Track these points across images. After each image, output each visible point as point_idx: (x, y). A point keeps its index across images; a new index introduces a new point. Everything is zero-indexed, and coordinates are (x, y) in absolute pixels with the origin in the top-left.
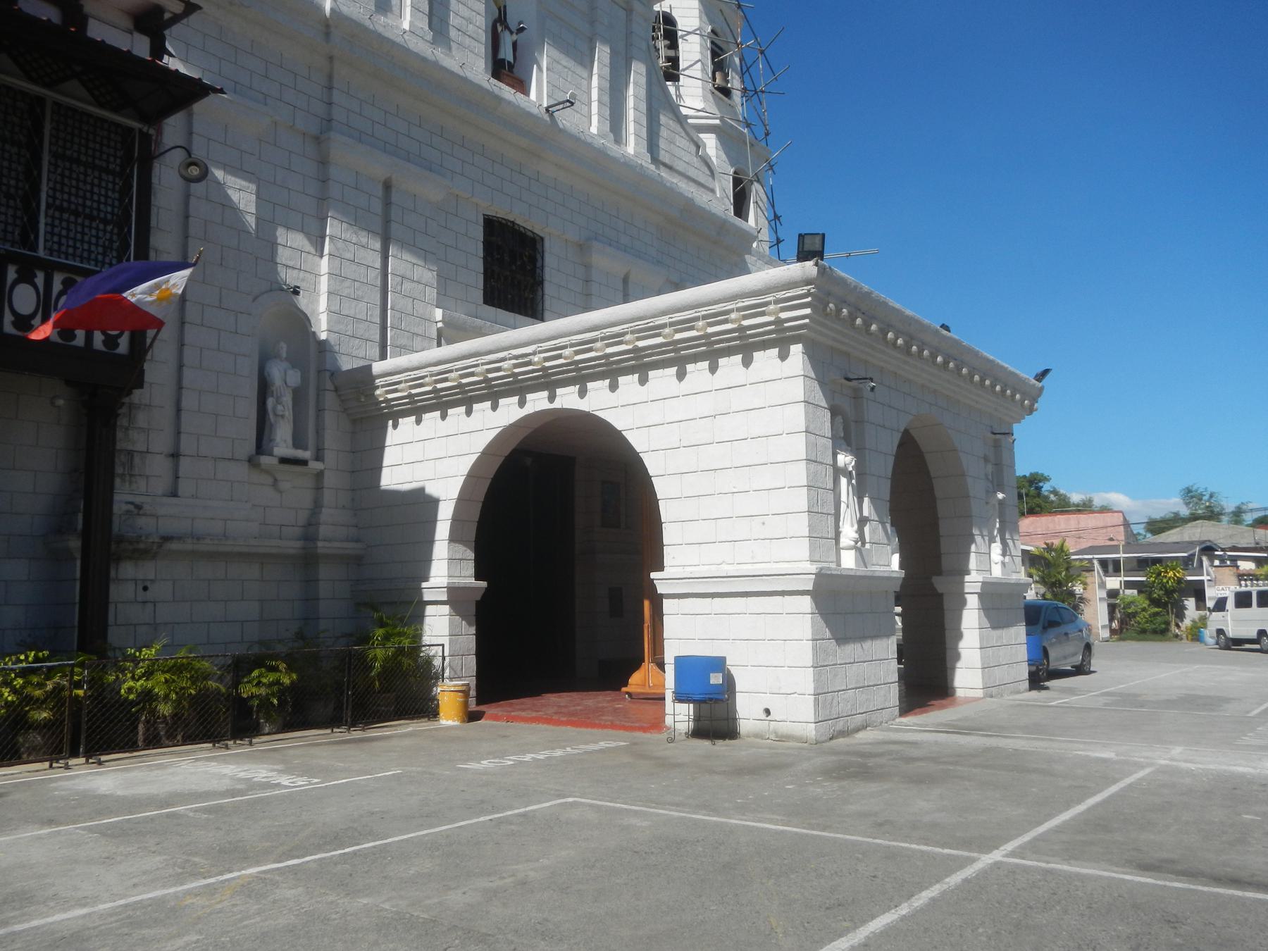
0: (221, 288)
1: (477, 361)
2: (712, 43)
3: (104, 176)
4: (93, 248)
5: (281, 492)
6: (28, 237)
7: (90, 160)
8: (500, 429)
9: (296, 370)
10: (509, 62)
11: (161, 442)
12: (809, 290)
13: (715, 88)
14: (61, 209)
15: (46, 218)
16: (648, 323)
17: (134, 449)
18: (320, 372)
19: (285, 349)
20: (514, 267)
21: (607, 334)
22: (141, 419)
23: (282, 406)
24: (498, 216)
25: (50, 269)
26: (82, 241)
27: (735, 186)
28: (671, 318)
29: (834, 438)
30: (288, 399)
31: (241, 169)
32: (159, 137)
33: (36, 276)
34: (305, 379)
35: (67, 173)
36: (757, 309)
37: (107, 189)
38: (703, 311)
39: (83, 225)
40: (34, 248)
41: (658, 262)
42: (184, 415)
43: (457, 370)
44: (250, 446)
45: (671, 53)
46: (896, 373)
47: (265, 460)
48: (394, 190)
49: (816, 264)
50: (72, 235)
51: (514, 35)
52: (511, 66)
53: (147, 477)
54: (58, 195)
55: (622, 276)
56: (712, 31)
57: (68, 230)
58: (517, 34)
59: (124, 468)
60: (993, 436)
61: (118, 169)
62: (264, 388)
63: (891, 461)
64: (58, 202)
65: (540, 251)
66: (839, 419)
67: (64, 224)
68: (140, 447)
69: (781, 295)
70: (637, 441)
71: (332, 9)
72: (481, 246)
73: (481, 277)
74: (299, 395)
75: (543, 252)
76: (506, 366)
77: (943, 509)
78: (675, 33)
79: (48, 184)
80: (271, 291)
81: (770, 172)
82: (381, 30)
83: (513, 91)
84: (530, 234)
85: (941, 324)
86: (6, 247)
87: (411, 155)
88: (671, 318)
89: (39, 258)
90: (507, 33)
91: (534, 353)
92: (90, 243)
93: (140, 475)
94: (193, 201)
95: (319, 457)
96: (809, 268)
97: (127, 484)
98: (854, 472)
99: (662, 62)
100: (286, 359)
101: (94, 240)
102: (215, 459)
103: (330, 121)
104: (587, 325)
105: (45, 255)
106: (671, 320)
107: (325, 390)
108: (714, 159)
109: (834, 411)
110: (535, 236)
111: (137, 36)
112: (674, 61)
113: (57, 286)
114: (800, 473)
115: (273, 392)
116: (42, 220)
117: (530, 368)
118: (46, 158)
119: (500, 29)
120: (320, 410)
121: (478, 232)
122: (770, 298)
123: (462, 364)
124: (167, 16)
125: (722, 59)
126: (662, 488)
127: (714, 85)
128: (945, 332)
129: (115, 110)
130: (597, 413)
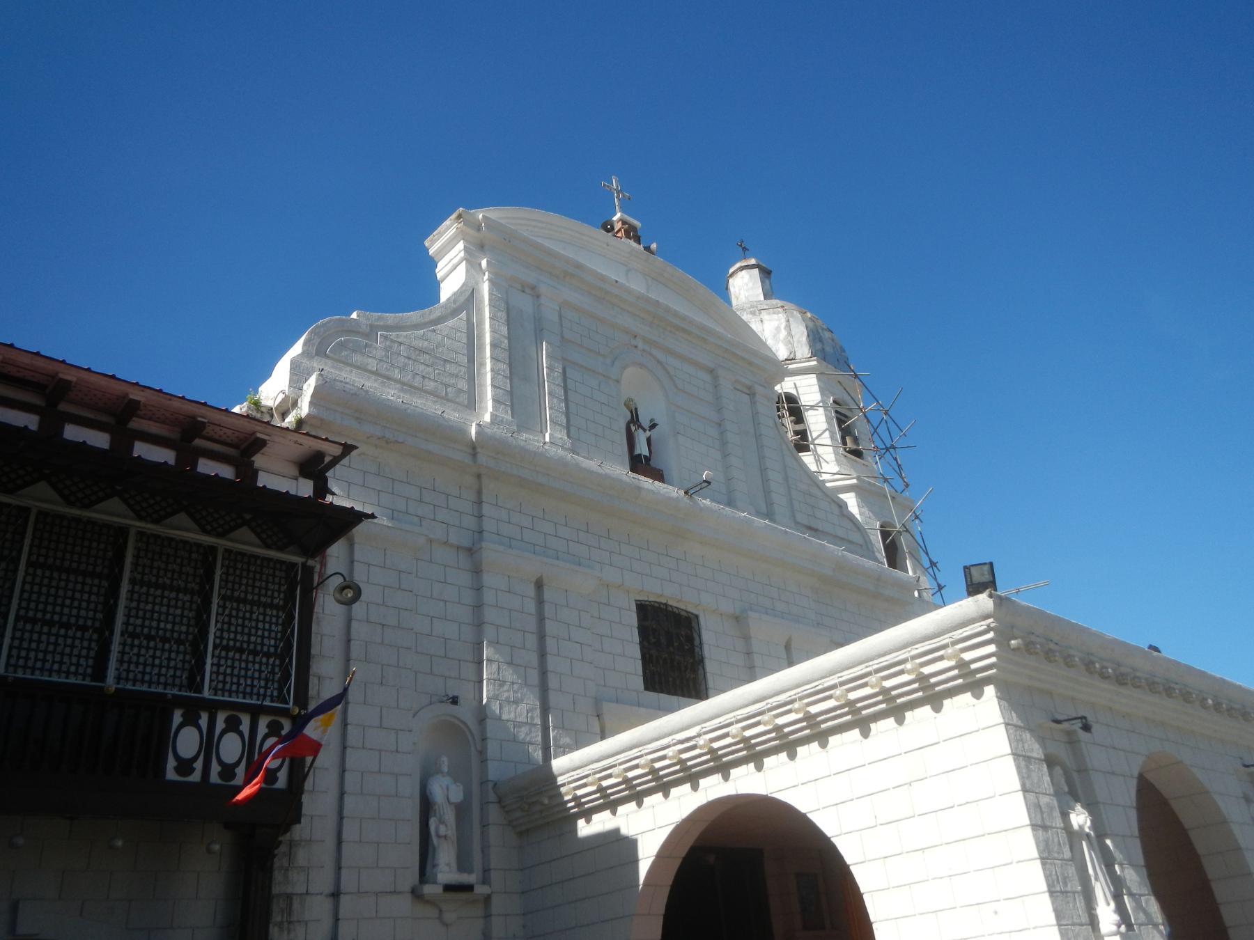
0: (381, 708)
1: (640, 751)
2: (837, 412)
3: (269, 612)
4: (256, 682)
5: (446, 925)
7: (256, 598)
8: (673, 826)
9: (458, 784)
10: (645, 456)
11: (322, 881)
12: (988, 626)
13: (848, 452)
14: (227, 648)
15: (212, 658)
16: (816, 686)
17: (294, 892)
18: (483, 783)
19: (446, 763)
20: (671, 649)
21: (774, 704)
22: (301, 857)
23: (444, 826)
24: (650, 600)
25: (213, 707)
26: (246, 677)
27: (884, 540)
28: (841, 677)
29: (1057, 794)
30: (450, 816)
31: (400, 588)
32: (323, 569)
33: (200, 717)
35: (234, 613)
36: (934, 654)
37: (271, 623)
38: (875, 665)
39: (247, 662)
40: (199, 689)
41: (818, 624)
42: (345, 847)
43: (621, 764)
44: (412, 876)
45: (799, 427)
46: (1110, 709)
47: (428, 889)
48: (545, 588)
49: (991, 596)
50: (236, 672)
51: (647, 432)
52: (648, 459)
53: (306, 923)
54: (225, 635)
55: (784, 644)
56: (835, 402)
57: (233, 667)
58: (650, 430)
59: (283, 916)
60: (1246, 769)
61: (281, 602)
62: (426, 807)
63: (1133, 814)
64: (225, 642)
65: (697, 629)
66: (1058, 770)
67: (229, 663)
68: (300, 889)
69: (958, 634)
70: (826, 823)
71: (476, 433)
72: (636, 632)
73: (639, 664)
74: (462, 811)
75: (699, 629)
76: (671, 754)
77: (1212, 868)
78: (799, 409)
79: (216, 626)
80: (431, 704)
81: (917, 521)
82: (522, 444)
83: (651, 481)
84: (683, 613)
85: (1148, 645)
86: (172, 692)
87: (559, 553)
88: (841, 677)
89: (204, 699)
90: (640, 431)
91: (699, 735)
92: (253, 678)
93: (299, 921)
94: (354, 624)
95: (485, 881)
96: (983, 601)
97: (286, 932)
98: (1092, 833)
99: (790, 436)
100: (449, 774)
101: (256, 675)
102: (377, 894)
103: (481, 532)
104: (751, 698)
105: (210, 695)
106: (841, 679)
107: (488, 802)
108: (858, 516)
109: (1051, 762)
110: (690, 614)
111: (301, 480)
112: (803, 434)
113: (220, 725)
114: (1026, 844)
115: (435, 810)
116: (209, 661)
117: (697, 752)
118: (215, 600)
119: (633, 428)
120: (484, 826)
121: (632, 619)
122: (945, 639)
123: (626, 757)
124: (327, 459)
125: (848, 425)
126: (864, 878)
127: (845, 449)
128: (1156, 654)
129: (280, 549)
130: (775, 796)
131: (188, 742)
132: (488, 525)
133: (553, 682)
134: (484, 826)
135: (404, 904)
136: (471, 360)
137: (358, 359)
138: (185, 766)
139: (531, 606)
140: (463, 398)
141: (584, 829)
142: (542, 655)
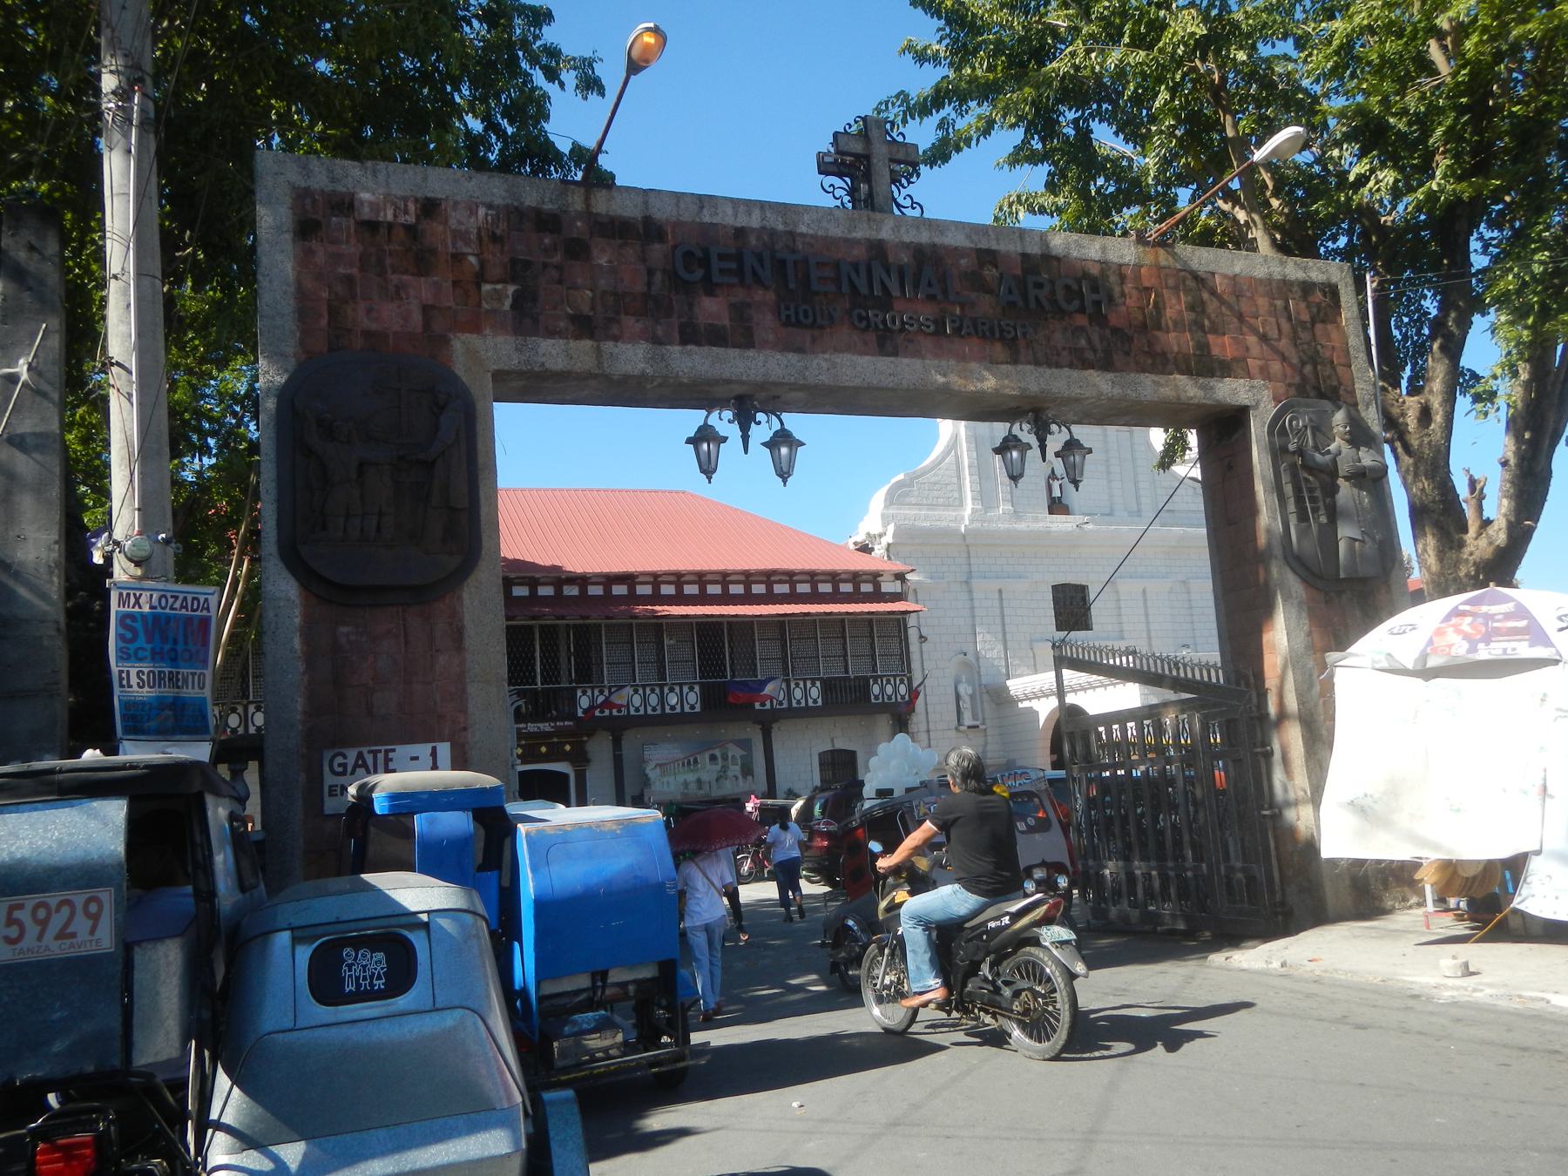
6: (875, 670)
18: (980, 685)
23: (966, 705)
30: (967, 699)
34: (974, 690)
47: (961, 728)
62: (958, 697)
74: (972, 697)
120: (982, 702)
131: (876, 689)
132: (974, 568)
133: (1008, 636)
134: (982, 702)
135: (953, 733)
136: (959, 478)
137: (907, 500)
138: (877, 697)
139: (997, 603)
140: (957, 503)
141: (1020, 705)
142: (1003, 625)
